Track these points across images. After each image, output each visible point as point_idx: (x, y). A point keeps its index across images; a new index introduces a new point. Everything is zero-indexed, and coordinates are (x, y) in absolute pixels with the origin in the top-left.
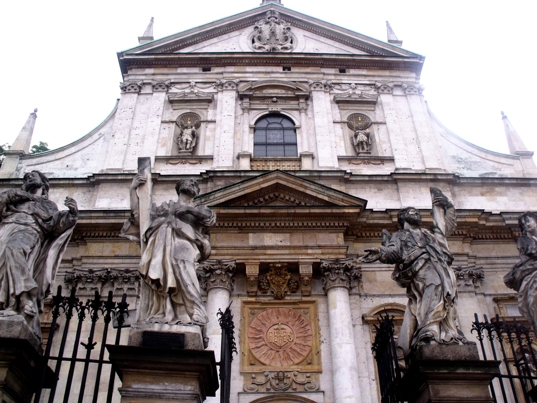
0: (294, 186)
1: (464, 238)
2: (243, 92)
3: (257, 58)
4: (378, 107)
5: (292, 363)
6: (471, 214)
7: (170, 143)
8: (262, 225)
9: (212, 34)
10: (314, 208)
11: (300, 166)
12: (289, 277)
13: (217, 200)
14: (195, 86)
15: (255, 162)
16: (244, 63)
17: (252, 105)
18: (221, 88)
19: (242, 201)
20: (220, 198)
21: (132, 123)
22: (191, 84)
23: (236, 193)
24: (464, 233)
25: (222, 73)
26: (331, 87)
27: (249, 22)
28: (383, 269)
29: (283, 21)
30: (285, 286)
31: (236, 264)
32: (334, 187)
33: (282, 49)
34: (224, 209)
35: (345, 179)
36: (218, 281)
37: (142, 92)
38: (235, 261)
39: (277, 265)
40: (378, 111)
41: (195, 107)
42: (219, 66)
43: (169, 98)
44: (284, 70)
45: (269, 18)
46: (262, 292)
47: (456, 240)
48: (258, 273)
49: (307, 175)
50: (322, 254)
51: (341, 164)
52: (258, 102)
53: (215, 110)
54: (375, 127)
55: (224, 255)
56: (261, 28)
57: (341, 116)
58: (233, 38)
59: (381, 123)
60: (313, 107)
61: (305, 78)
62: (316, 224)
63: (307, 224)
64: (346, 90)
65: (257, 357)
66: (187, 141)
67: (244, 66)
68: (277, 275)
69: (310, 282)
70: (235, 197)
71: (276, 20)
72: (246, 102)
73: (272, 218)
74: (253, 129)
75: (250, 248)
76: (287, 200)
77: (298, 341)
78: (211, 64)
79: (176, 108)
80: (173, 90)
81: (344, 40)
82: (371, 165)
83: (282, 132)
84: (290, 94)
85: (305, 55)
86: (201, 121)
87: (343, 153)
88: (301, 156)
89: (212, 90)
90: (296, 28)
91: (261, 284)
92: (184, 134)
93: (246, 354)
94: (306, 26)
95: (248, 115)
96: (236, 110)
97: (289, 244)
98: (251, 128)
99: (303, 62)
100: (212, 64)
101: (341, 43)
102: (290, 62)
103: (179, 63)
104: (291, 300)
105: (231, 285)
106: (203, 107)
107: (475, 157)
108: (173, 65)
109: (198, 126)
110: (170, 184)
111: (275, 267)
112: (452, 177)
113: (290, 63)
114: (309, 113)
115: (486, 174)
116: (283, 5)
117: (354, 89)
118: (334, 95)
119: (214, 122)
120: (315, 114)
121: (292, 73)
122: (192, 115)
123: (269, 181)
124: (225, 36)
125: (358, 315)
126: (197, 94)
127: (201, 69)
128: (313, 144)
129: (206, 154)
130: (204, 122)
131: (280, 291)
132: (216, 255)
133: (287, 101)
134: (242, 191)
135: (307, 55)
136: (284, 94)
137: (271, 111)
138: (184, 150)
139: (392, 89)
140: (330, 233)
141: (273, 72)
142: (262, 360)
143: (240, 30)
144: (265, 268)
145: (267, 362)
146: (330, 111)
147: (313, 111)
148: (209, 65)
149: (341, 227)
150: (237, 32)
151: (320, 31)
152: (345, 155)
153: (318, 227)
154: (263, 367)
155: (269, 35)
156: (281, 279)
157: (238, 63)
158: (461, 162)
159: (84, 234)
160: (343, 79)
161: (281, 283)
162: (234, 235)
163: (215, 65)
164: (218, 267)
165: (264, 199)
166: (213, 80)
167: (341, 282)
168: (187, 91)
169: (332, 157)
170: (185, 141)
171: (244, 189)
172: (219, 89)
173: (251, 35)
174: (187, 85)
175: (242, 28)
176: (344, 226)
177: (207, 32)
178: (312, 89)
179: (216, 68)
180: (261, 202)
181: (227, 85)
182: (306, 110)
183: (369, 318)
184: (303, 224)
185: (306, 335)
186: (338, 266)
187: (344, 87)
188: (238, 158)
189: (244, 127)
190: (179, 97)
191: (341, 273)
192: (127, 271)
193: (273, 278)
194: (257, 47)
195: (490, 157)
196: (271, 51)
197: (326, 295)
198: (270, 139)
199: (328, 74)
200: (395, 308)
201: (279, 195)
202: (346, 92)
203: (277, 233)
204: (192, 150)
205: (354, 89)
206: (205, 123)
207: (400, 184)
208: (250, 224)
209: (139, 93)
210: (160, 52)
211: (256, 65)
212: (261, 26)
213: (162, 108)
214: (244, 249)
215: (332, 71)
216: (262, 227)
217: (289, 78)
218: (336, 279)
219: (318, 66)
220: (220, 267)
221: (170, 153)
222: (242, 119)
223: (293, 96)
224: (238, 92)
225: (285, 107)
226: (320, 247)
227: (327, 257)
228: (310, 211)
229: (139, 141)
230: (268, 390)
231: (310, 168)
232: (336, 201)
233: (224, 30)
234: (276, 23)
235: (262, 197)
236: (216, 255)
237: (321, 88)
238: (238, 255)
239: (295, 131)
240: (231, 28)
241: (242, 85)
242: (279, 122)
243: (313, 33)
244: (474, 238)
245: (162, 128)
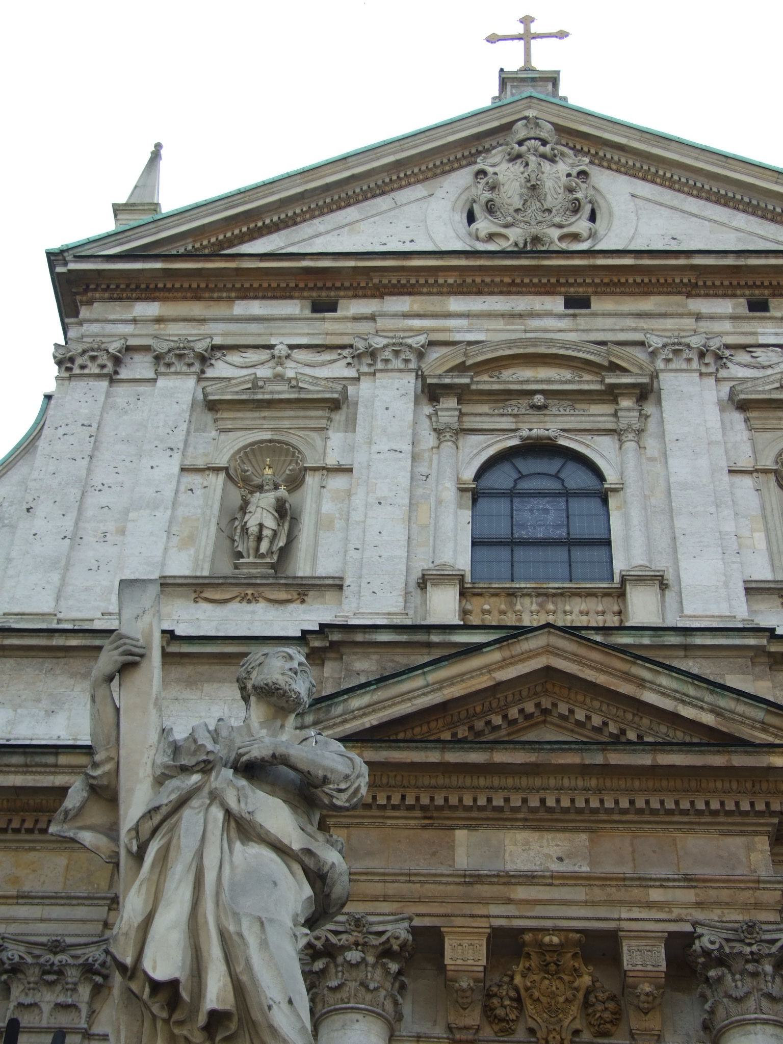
0: (601, 679)
2: (440, 375)
3: (480, 268)
7: (208, 536)
8: (498, 802)
9: (343, 195)
10: (669, 752)
11: (620, 613)
12: (586, 980)
13: (355, 718)
14: (288, 357)
15: (477, 601)
16: (441, 285)
17: (465, 419)
18: (370, 365)
19: (433, 725)
20: (365, 714)
21: (89, 471)
22: (276, 352)
23: (415, 698)
25: (372, 318)
26: (721, 358)
27: (459, 156)
29: (565, 150)
30: (574, 1009)
31: (414, 930)
32: (733, 681)
33: (562, 238)
34: (376, 749)
35: (770, 655)
36: (353, 985)
37: (124, 374)
38: (411, 919)
39: (547, 939)
41: (287, 424)
42: (365, 296)
43: (205, 395)
44: (567, 305)
45: (520, 143)
46: (496, 1028)
48: (484, 962)
49: (646, 641)
50: (700, 905)
51: (756, 607)
52: (485, 409)
53: (350, 435)
55: (374, 899)
56: (496, 174)
57: (754, 452)
58: (406, 208)
60: (662, 421)
61: (635, 330)
62: (677, 803)
63: (647, 802)
64: (770, 366)
66: (261, 531)
68: (548, 973)
69: (658, 1001)
70: (410, 710)
71: (542, 149)
72: (447, 409)
73: (531, 781)
74: (470, 494)
75: (457, 880)
76: (578, 723)
78: (338, 289)
79: (229, 425)
80: (220, 369)
81: (762, 205)
83: (563, 505)
84: (588, 382)
85: (635, 258)
86: (306, 469)
88: (623, 580)
89: (340, 370)
90: (608, 172)
91: (495, 1001)
92: (251, 508)
94: (638, 165)
95: (454, 451)
96: (414, 434)
97: (586, 869)
98: (462, 490)
99: (631, 280)
100: (342, 288)
101: (753, 214)
102: (588, 280)
103: (238, 285)
105: (396, 1003)
108: (220, 290)
109: (295, 482)
110: (203, 664)
111: (540, 945)
113: (589, 285)
116: (565, 99)
118: (732, 384)
119: (350, 470)
120: (669, 446)
121: (595, 315)
123: (521, 661)
124: (383, 203)
126: (294, 383)
127: (308, 304)
128: (663, 543)
129: (321, 571)
130: (315, 469)
131: (558, 1028)
133: (577, 406)
134: (433, 691)
135: (642, 258)
136: (567, 382)
137: (528, 438)
138: (251, 560)
141: (532, 315)
143: (427, 183)
146: (718, 436)
147: (663, 436)
148: (332, 294)
149: (760, 814)
150: (419, 186)
151: (683, 180)
152: (770, 577)
153: (685, 813)
155: (521, 195)
156: (561, 986)
157: (422, 286)
160: (760, 330)
161: (561, 999)
162: (407, 832)
163: (350, 293)
164: (352, 939)
165: (505, 717)
166: (346, 340)
167: (765, 1003)
168: (264, 372)
169: (726, 585)
170: (253, 529)
171: (441, 685)
172: (365, 369)
173: (464, 197)
174: (264, 355)
175: (436, 176)
176: (772, 814)
177: (327, 188)
178: (660, 365)
179: (354, 301)
180: (497, 728)
181: (387, 354)
182: (640, 432)
184: (632, 802)
186: (755, 948)
187: (764, 356)
188: (423, 583)
189: (440, 488)
190: (237, 393)
191: (765, 975)
193: (533, 982)
194: (483, 234)
196: (529, 248)
198: (523, 526)
199: (712, 318)
201: (555, 705)
202: (769, 372)
203: (548, 830)
204: (275, 557)
206: (318, 475)
208: (461, 800)
209: (112, 379)
210: (182, 251)
211: (479, 293)
212: (496, 169)
213: (185, 426)
214: (440, 883)
215: (725, 306)
216: (500, 809)
217: (583, 331)
218: (748, 994)
219: (679, 293)
220: (361, 941)
222: (435, 462)
224: (421, 376)
225: (571, 422)
226: (690, 881)
227: (714, 915)
228: (654, 759)
229: (111, 527)
231: (653, 620)
232: (741, 727)
233: (380, 183)
234: (543, 156)
235: (497, 713)
237: (689, 360)
238: (420, 900)
239: (605, 502)
240: (402, 175)
241: (435, 354)
242: (553, 472)
243: (661, 185)
245: (182, 488)
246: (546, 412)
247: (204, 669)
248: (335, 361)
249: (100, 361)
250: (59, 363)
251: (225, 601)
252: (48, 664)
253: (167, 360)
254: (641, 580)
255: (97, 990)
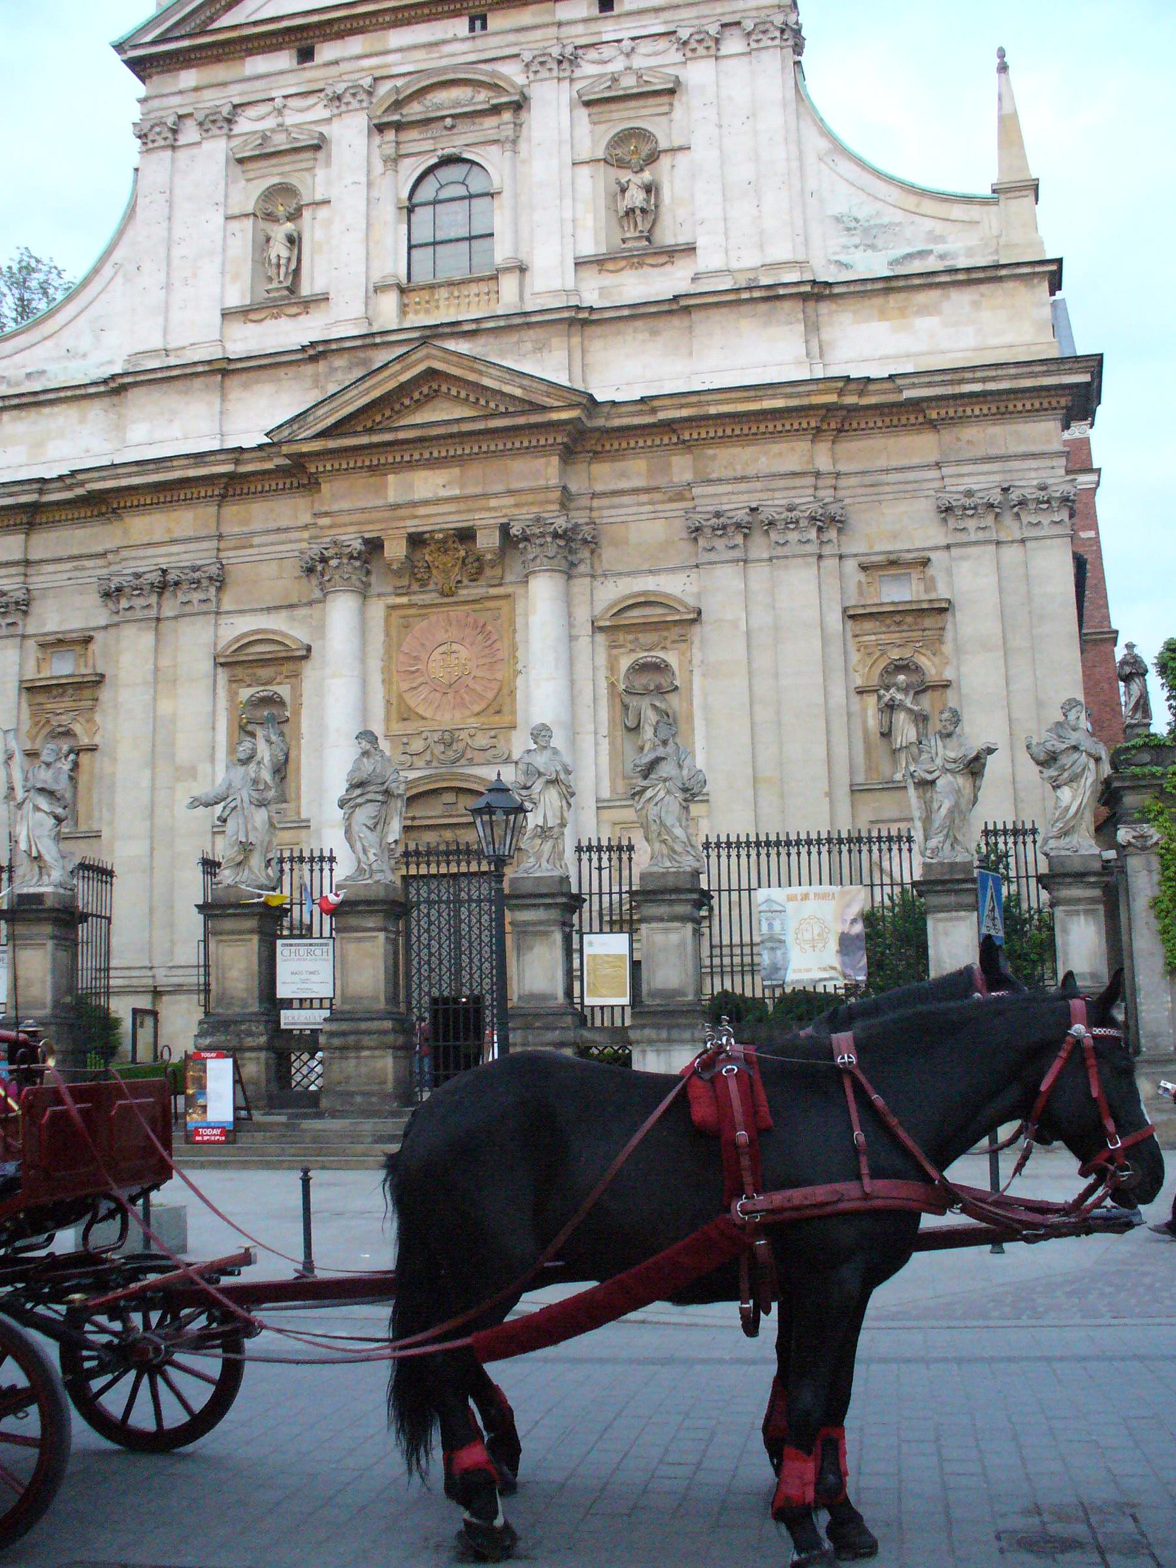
1: (815, 436)
2: (380, 117)
4: (680, 100)
5: (468, 713)
6: (821, 386)
14: (285, 106)
15: (412, 294)
18: (338, 107)
21: (170, 229)
24: (813, 424)
25: (337, 63)
28: (643, 517)
36: (337, 577)
37: (183, 139)
40: (677, 114)
41: (287, 168)
42: (332, 40)
44: (472, 29)
47: (798, 440)
50: (516, 505)
54: (665, 161)
55: (345, 525)
59: (680, 149)
60: (530, 128)
61: (516, 44)
65: (413, 705)
67: (384, 29)
77: (480, 674)
78: (312, 38)
79: (251, 175)
80: (244, 125)
82: (647, 269)
87: (588, 248)
92: (272, 242)
93: (394, 701)
97: (457, 492)
104: (468, 595)
106: (304, 165)
107: (892, 210)
112: (808, 288)
114: (523, 146)
115: (910, 256)
117: (628, 55)
122: (284, 190)
125: (583, 615)
127: (294, 53)
130: (308, 205)
132: (331, 527)
133: (477, 120)
138: (275, 285)
139: (717, 41)
140: (537, 457)
141: (444, 42)
142: (420, 711)
144: (416, 541)
145: (428, 714)
148: (309, 41)
154: (422, 723)
158: (855, 229)
159: (115, 506)
160: (603, 29)
167: (545, 560)
168: (270, 123)
169: (562, 262)
170: (274, 261)
172: (336, 111)
182: (515, 142)
183: (602, 624)
185: (494, 660)
187: (607, 52)
192: (195, 569)
195: (929, 206)
197: (527, 582)
200: (652, 599)
205: (628, 55)
206: (310, 208)
207: (696, 316)
209: (174, 148)
213: (223, 184)
221: (248, 295)
223: (486, 106)
226: (511, 492)
230: (428, 763)
236: (331, 527)
237: (550, 70)
244: (840, 431)
245: (229, 234)
246: (455, 131)
247: (252, 374)
248: (316, 104)
249: (164, 135)
250: (139, 137)
251: (261, 320)
252: (165, 386)
253: (205, 127)
254: (507, 270)
255: (219, 589)
